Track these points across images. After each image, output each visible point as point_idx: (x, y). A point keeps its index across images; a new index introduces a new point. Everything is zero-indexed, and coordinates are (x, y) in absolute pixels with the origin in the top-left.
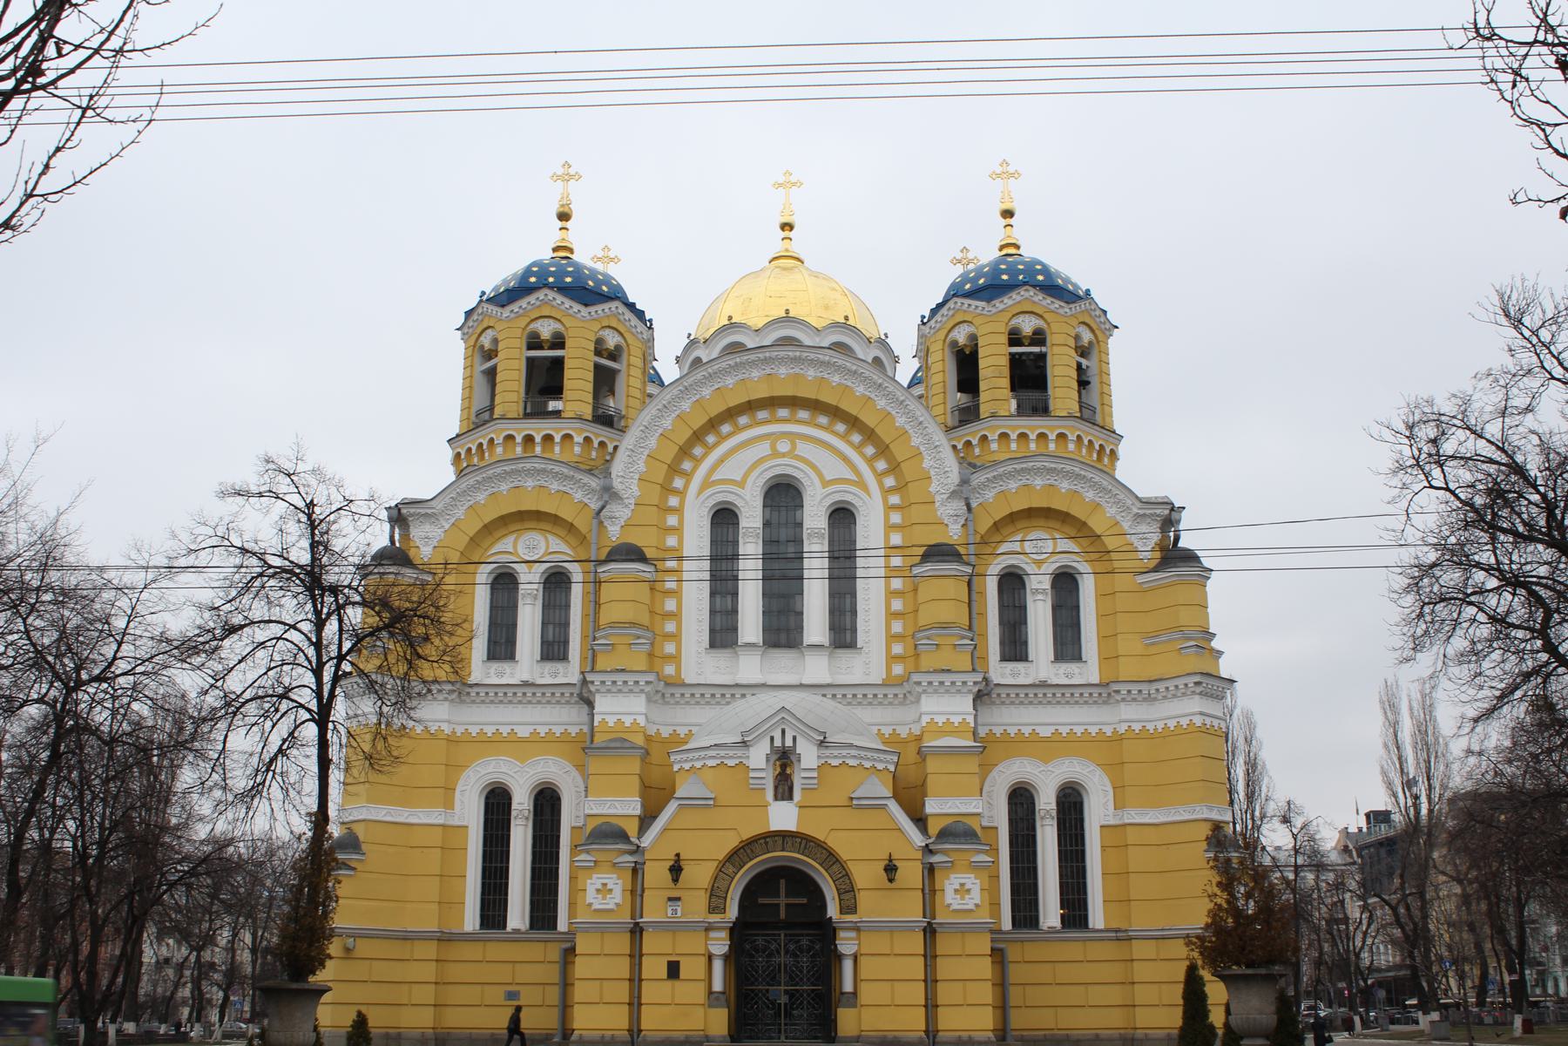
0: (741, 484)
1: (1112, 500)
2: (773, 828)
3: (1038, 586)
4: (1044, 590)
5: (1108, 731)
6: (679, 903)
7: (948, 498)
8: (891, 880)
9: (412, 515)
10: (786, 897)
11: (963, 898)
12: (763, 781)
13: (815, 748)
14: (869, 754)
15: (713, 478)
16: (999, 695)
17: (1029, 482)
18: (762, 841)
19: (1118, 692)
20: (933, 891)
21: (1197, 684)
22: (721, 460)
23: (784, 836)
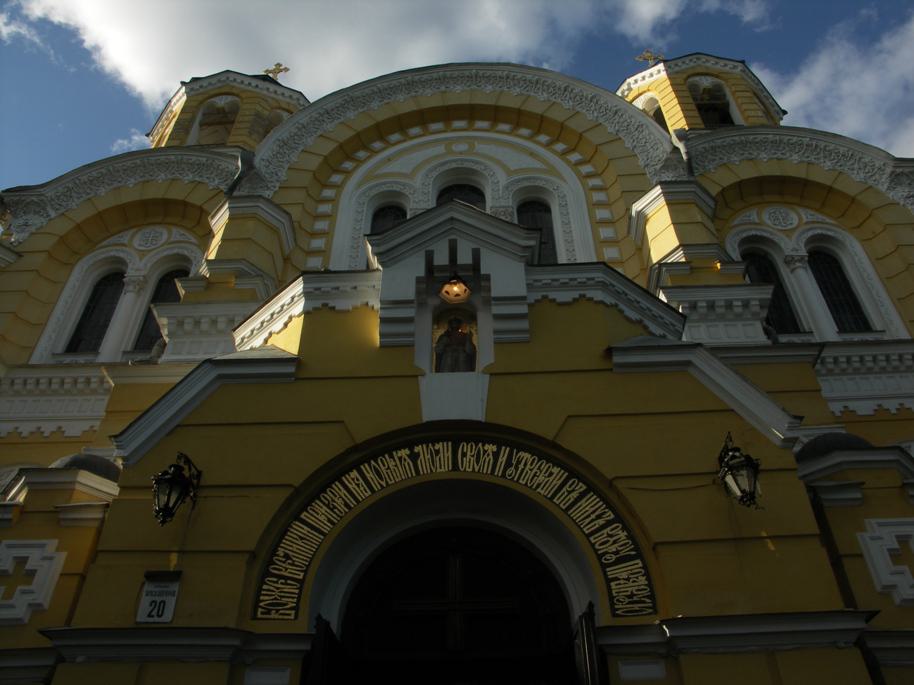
1: (856, 166)
2: (429, 414)
3: (794, 253)
4: (802, 258)
6: (175, 587)
7: (660, 169)
13: (521, 266)
15: (379, 172)
18: (404, 452)
22: (389, 159)
23: (457, 432)
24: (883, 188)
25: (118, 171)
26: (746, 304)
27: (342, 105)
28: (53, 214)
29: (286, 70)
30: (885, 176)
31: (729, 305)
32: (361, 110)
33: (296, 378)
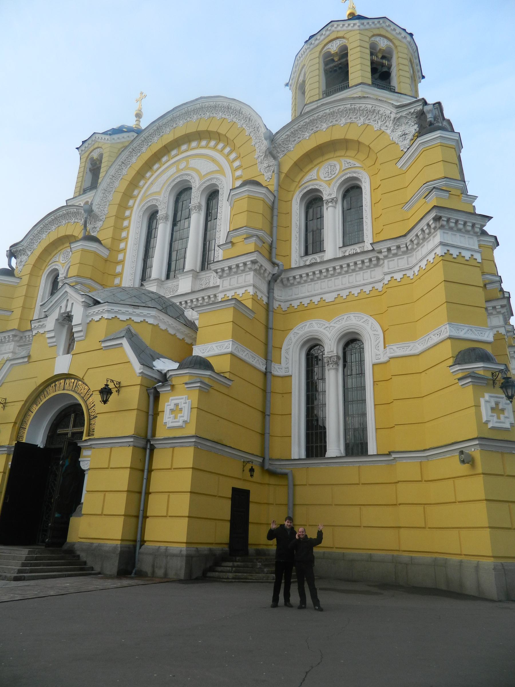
0: (158, 193)
1: (377, 118)
2: (56, 373)
4: (333, 199)
5: (379, 286)
8: (105, 402)
9: (16, 251)
10: (74, 426)
11: (175, 418)
12: (54, 340)
14: (123, 309)
16: (294, 277)
17: (318, 129)
19: (380, 252)
20: (156, 414)
21: (437, 219)
22: (152, 183)
24: (389, 131)
25: (47, 224)
26: (245, 264)
27: (129, 156)
28: (29, 253)
29: (145, 96)
30: (391, 122)
31: (237, 266)
32: (139, 154)
33: (28, 362)
